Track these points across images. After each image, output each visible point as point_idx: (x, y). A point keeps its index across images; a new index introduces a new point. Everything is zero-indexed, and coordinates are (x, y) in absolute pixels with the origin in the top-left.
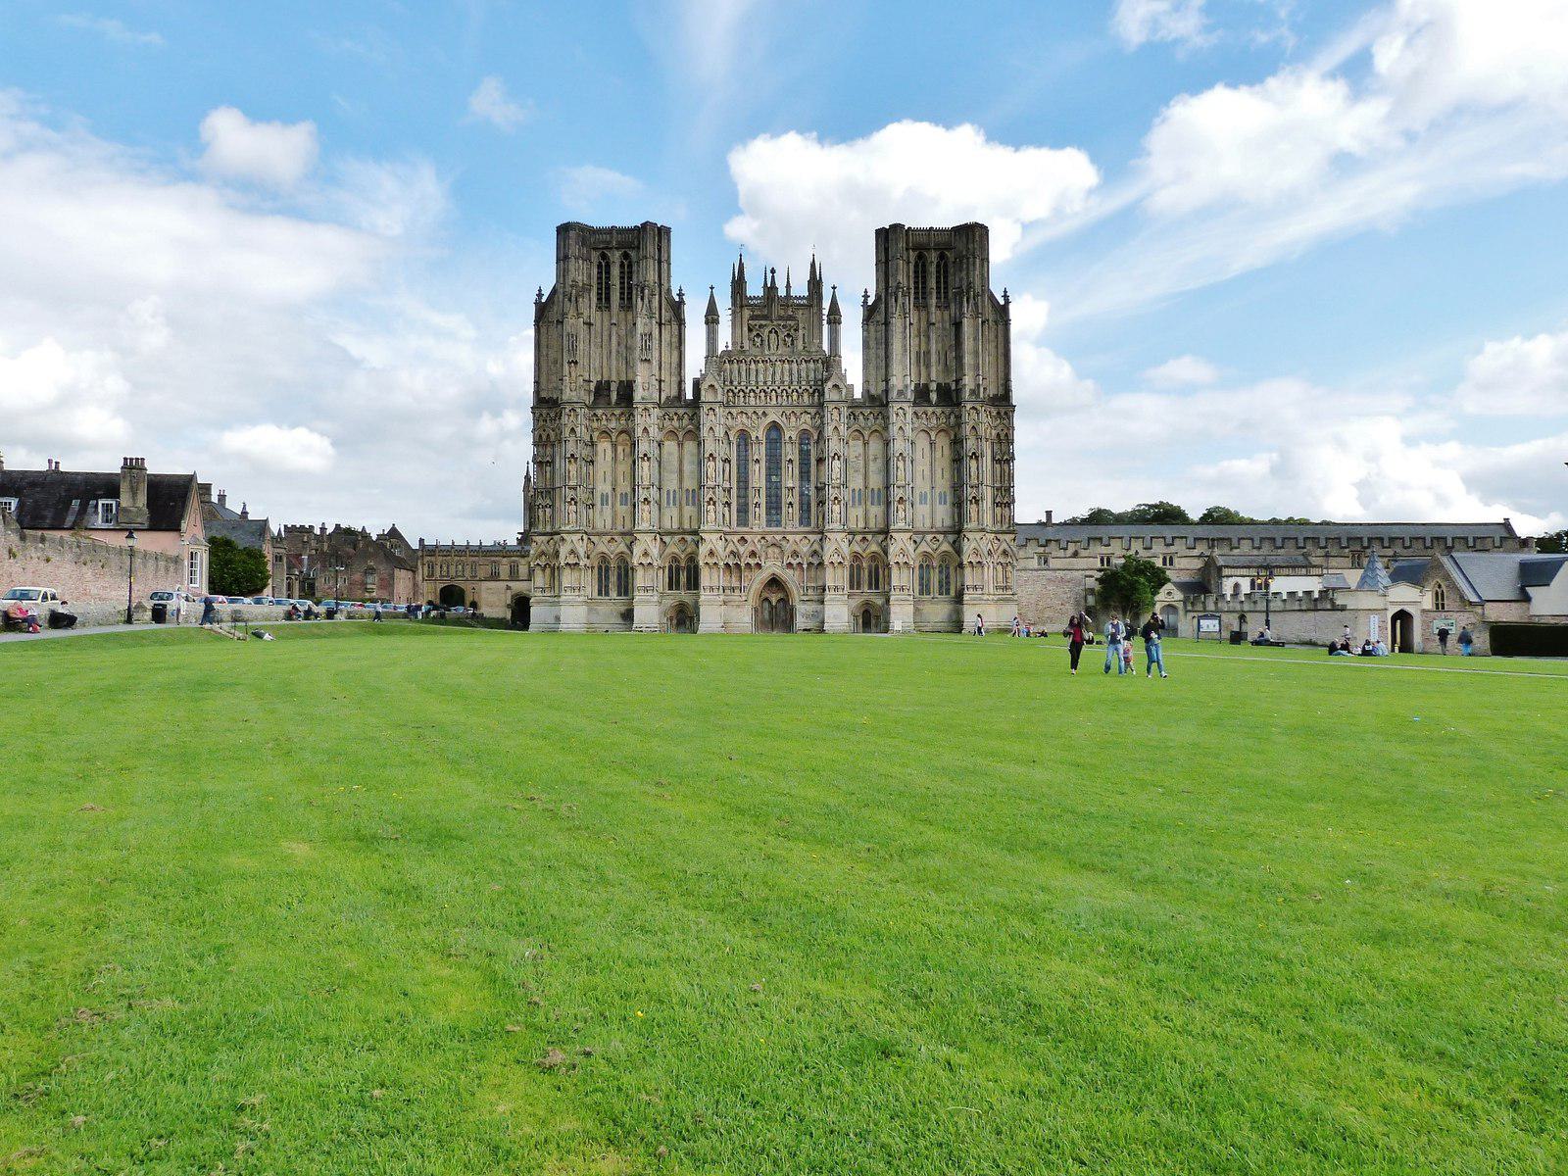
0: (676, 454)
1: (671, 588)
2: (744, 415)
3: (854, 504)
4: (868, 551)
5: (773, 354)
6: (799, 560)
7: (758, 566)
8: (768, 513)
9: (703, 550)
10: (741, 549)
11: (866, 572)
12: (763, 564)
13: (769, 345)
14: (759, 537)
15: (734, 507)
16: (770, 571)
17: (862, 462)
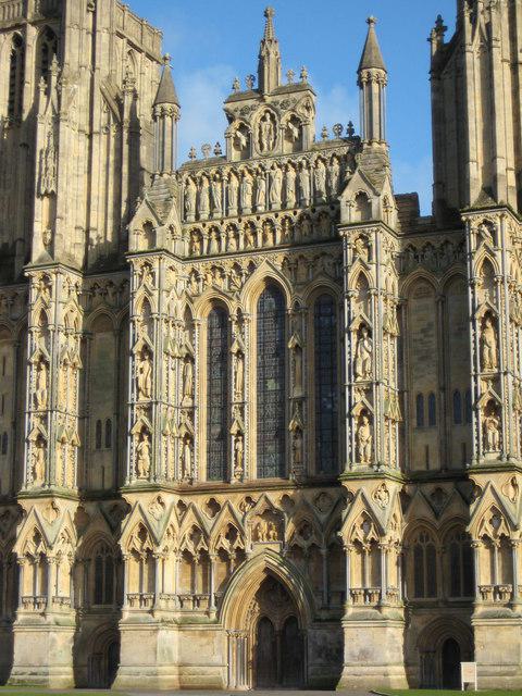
0: (112, 356)
1: (98, 601)
2: (218, 274)
3: (420, 423)
4: (443, 517)
5: (266, 157)
6: (313, 539)
7: (241, 555)
8: (262, 452)
9: (130, 526)
10: (208, 522)
11: (446, 557)
12: (248, 550)
13: (260, 142)
14: (241, 497)
15: (201, 440)
16: (262, 564)
17: (433, 342)
